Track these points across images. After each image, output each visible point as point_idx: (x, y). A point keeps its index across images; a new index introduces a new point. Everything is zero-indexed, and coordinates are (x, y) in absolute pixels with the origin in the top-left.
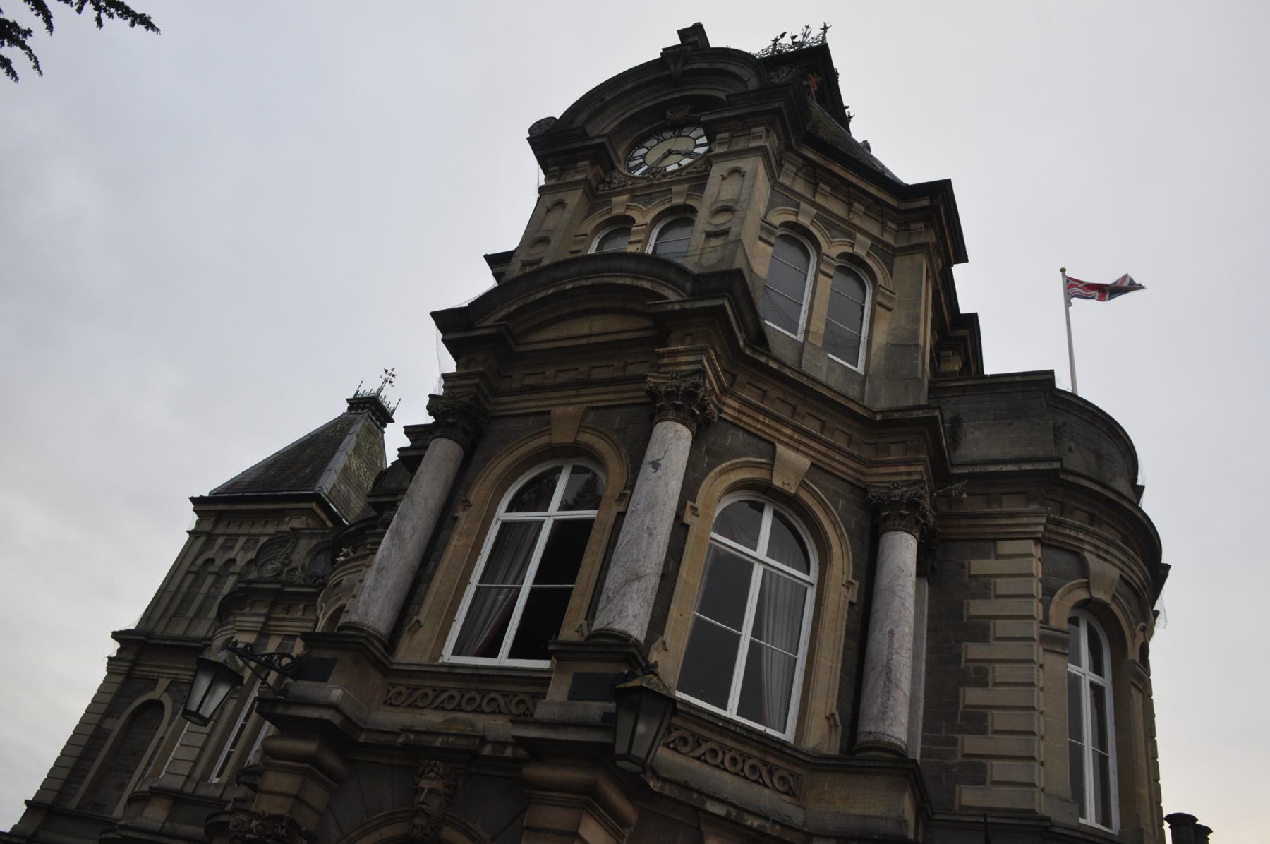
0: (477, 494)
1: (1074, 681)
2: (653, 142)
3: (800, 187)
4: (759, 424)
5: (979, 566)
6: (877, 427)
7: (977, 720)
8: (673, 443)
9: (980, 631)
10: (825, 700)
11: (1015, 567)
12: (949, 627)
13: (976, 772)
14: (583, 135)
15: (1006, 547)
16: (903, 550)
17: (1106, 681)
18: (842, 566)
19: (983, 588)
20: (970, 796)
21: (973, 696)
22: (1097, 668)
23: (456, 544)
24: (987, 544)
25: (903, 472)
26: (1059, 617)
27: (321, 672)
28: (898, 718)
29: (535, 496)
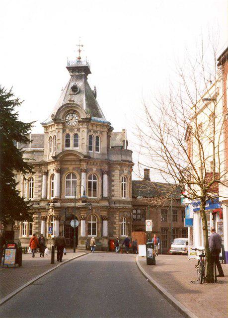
0: (63, 179)
1: (122, 184)
2: (68, 116)
3: (90, 127)
4: (90, 167)
5: (113, 173)
6: (102, 162)
7: (113, 191)
8: (83, 174)
9: (113, 181)
10: (100, 193)
11: (116, 173)
12: (110, 181)
13: (113, 196)
14: (60, 120)
15: (115, 171)
16: (105, 177)
17: (126, 183)
18: (100, 179)
19: (114, 176)
20: (113, 198)
21: (113, 188)
22: (125, 181)
23: (63, 184)
24: (114, 171)
25: (105, 168)
26: (121, 180)
27: (56, 202)
28: (106, 195)
29: (68, 177)
